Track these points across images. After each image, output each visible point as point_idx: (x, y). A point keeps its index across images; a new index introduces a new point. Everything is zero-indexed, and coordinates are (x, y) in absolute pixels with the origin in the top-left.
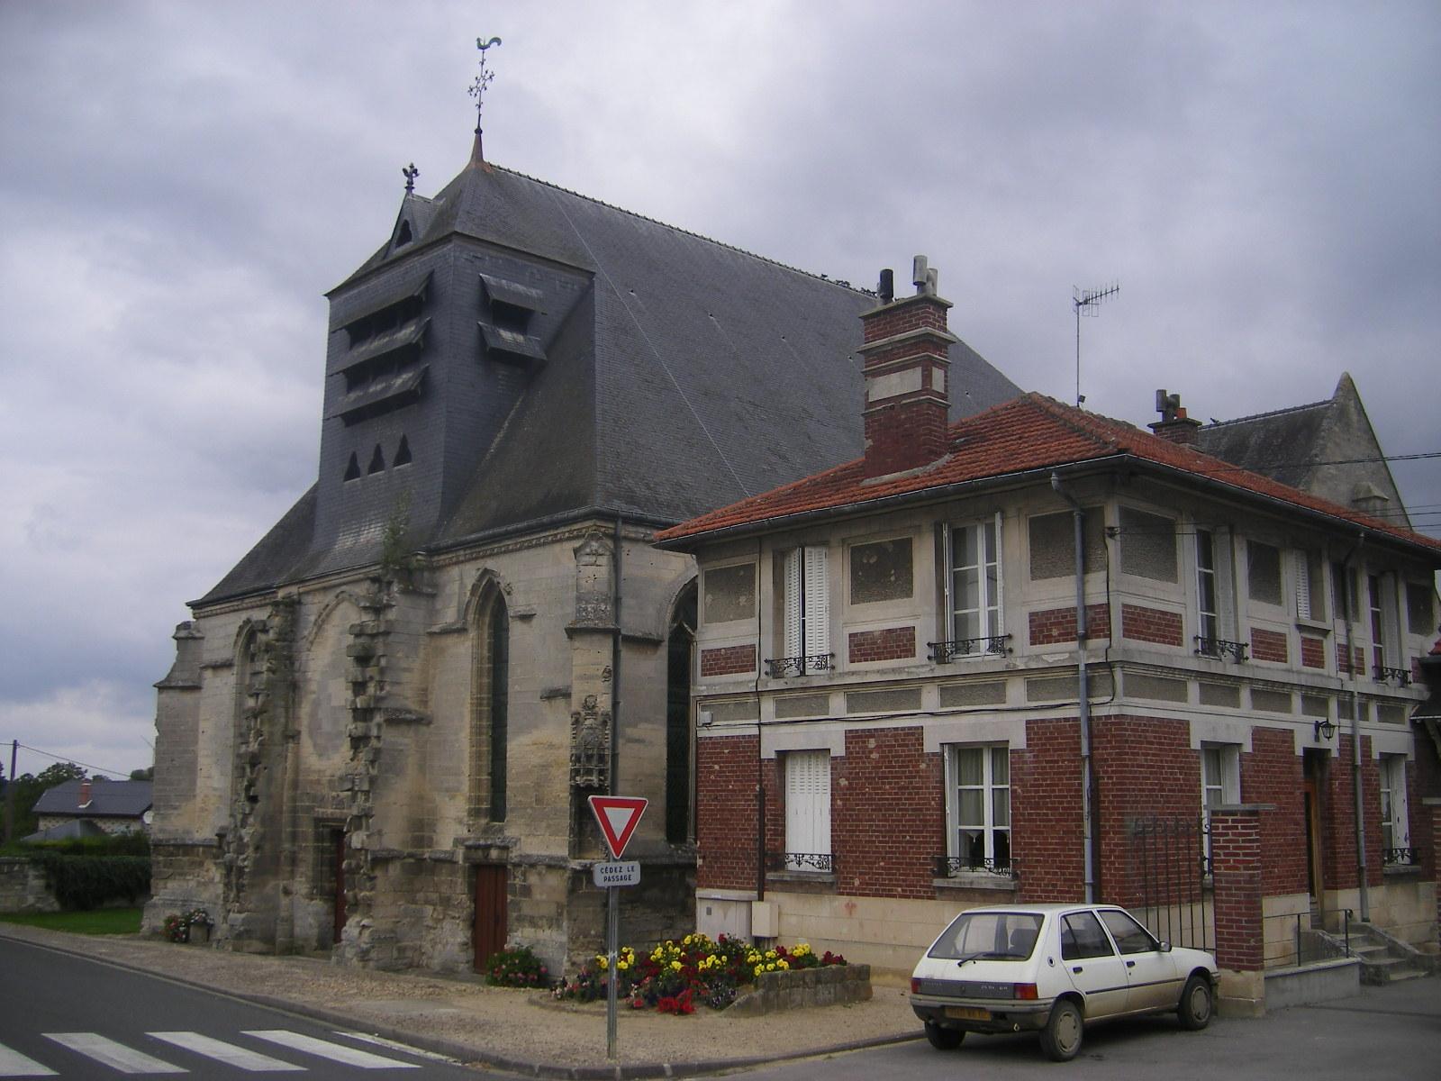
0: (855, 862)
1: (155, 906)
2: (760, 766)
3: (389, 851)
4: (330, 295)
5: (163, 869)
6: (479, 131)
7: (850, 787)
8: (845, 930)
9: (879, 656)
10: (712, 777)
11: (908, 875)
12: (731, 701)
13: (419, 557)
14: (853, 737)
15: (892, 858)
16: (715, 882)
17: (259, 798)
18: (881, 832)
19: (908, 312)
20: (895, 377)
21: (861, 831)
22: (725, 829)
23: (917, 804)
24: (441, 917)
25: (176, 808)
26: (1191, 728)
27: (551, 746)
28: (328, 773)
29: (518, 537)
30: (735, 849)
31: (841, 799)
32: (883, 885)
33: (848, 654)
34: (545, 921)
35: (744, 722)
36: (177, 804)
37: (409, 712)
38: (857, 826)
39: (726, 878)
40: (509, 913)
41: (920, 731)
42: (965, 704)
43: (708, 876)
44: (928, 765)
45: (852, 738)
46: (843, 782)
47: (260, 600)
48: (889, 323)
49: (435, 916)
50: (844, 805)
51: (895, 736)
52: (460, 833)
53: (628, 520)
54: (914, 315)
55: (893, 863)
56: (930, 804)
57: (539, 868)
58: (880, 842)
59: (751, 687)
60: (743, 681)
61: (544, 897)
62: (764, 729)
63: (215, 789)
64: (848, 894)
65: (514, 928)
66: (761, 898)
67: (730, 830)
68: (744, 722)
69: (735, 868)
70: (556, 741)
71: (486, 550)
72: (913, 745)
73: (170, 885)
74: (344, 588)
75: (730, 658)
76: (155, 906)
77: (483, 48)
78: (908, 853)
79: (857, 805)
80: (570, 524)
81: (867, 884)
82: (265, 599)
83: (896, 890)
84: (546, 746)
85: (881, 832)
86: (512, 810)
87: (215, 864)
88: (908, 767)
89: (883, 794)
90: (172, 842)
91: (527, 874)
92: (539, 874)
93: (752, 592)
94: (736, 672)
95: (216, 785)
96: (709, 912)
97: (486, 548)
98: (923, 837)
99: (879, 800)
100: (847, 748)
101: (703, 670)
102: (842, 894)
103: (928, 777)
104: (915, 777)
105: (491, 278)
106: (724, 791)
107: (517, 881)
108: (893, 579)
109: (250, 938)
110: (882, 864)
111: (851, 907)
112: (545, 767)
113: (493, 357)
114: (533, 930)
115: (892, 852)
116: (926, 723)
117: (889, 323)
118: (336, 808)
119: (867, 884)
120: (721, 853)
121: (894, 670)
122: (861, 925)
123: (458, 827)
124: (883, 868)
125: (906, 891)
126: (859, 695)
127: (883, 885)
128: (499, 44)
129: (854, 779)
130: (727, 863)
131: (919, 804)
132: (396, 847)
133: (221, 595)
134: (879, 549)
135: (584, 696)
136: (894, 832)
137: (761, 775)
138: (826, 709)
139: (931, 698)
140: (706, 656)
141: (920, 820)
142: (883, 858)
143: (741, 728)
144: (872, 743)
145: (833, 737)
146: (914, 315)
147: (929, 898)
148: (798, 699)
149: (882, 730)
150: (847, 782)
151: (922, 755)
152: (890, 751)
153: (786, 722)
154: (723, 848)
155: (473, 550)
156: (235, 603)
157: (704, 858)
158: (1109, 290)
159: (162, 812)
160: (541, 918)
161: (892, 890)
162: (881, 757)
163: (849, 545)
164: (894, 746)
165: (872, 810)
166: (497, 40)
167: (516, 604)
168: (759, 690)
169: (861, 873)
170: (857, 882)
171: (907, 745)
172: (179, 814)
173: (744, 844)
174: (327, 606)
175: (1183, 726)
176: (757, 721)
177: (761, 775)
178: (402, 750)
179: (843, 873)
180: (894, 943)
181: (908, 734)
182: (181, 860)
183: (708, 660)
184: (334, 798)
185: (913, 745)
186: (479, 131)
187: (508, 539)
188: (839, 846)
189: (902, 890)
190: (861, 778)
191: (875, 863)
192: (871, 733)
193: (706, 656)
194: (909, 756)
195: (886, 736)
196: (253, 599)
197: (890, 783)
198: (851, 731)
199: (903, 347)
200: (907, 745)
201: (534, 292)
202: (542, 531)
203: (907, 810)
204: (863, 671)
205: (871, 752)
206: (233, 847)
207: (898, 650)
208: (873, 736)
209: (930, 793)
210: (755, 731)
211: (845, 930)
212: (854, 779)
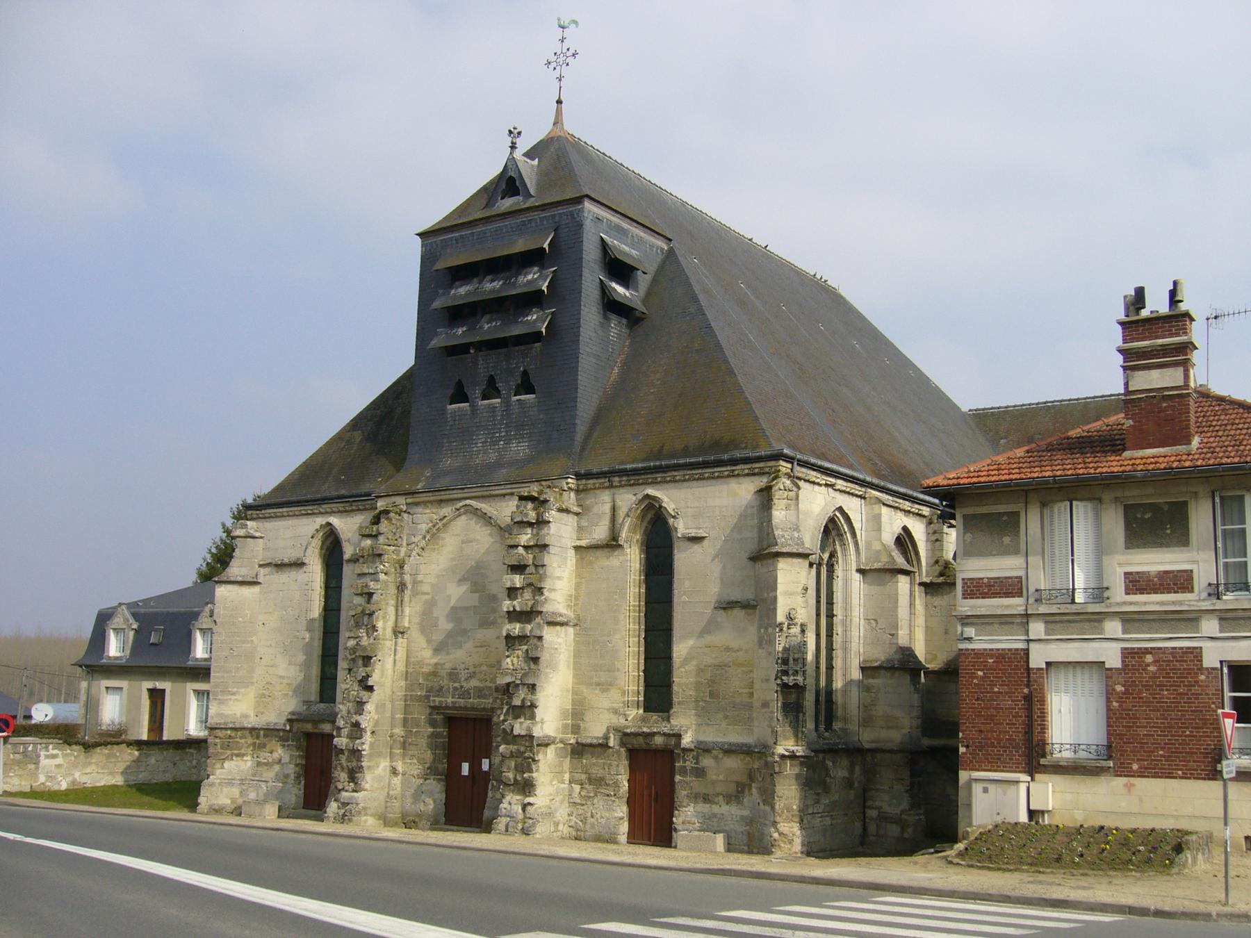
0: (1131, 751)
1: (212, 785)
2: (1028, 674)
3: (548, 737)
4: (421, 235)
5: (220, 751)
6: (559, 102)
7: (1126, 692)
8: (1123, 804)
9: (1155, 591)
10: (975, 681)
11: (1189, 761)
12: (996, 620)
13: (569, 480)
14: (1129, 653)
15: (1171, 748)
16: (980, 766)
17: (375, 688)
18: (1160, 727)
19: (1168, 323)
20: (1155, 373)
21: (1138, 727)
22: (990, 724)
23: (1196, 707)
24: (592, 795)
25: (234, 694)
26: (1204, 654)
27: (728, 649)
28: (448, 666)
29: (688, 469)
30: (1002, 740)
31: (1117, 702)
32: (1162, 769)
33: (1123, 588)
34: (721, 797)
35: (1010, 638)
36: (235, 690)
37: (561, 615)
38: (1134, 723)
39: (992, 762)
40: (677, 791)
41: (1199, 650)
42: (1244, 631)
43: (971, 762)
44: (1208, 677)
45: (1127, 654)
46: (1119, 688)
47: (344, 507)
48: (1147, 329)
49: (583, 794)
50: (1120, 706)
51: (1171, 653)
52: (613, 721)
53: (804, 464)
54: (1175, 326)
55: (1172, 752)
56: (1210, 707)
57: (715, 752)
58: (1158, 735)
59: (1021, 610)
60: (1014, 605)
61: (721, 777)
62: (1033, 646)
63: (281, 677)
64: (1125, 776)
65: (685, 804)
66: (1033, 780)
67: (995, 724)
68: (1010, 638)
69: (1002, 755)
70: (734, 645)
71: (638, 480)
72: (1191, 661)
73: (226, 764)
74: (468, 502)
75: (994, 586)
76: (212, 785)
77: (563, 27)
78: (1189, 744)
79: (1133, 706)
80: (752, 463)
81: (1146, 768)
82: (352, 505)
83: (1176, 773)
84: (722, 649)
85: (1160, 727)
86: (679, 703)
87: (283, 746)
88: (1187, 678)
89: (1160, 698)
90: (231, 726)
91: (700, 758)
92: (716, 758)
93: (1017, 533)
94: (1000, 597)
95: (281, 673)
96: (985, 790)
97: (649, 476)
98: (1204, 732)
99: (1157, 703)
100: (1123, 662)
101: (963, 594)
102: (1120, 776)
103: (1208, 686)
104: (1194, 686)
105: (608, 238)
106: (988, 693)
107: (688, 763)
108: (1168, 531)
109: (366, 814)
110: (1161, 752)
111: (1129, 787)
112: (720, 666)
113: (612, 306)
114: (708, 806)
115: (1172, 744)
116: (1206, 645)
117: (1147, 329)
118: (459, 698)
119: (1146, 768)
120: (986, 743)
121: (1174, 603)
122: (1141, 800)
123: (612, 716)
124: (1162, 756)
125: (1186, 774)
126: (1131, 620)
127: (1162, 769)
128: (577, 27)
129: (1129, 686)
130: (993, 751)
131: (1198, 707)
132: (552, 734)
133: (272, 501)
134: (1154, 507)
135: (787, 609)
136: (1173, 727)
137: (1029, 681)
138: (1102, 631)
139: (1210, 626)
140: (966, 583)
141: (1199, 719)
142: (1163, 749)
143: (1008, 642)
144: (1149, 658)
145: (1112, 656)
146: (1175, 326)
147: (1210, 779)
148: (1069, 621)
149: (1160, 649)
150: (1123, 689)
151: (1201, 669)
152: (1167, 665)
153: (1057, 639)
154: (988, 739)
155: (632, 478)
156: (310, 508)
157: (967, 747)
158: (1226, 313)
159: (219, 697)
160: (718, 795)
161: (1173, 773)
162: (1158, 670)
163: (1122, 502)
164: (1172, 661)
165: (1150, 710)
166: (575, 22)
167: (682, 527)
168: (1029, 613)
169: (1138, 760)
170: (1135, 767)
171: (1186, 661)
172: (236, 700)
173: (1012, 736)
174: (445, 517)
175: (1197, 654)
176: (1025, 638)
177: (1029, 681)
178: (556, 649)
179: (1120, 759)
180: (1175, 813)
181: (1186, 653)
182: (238, 742)
183: (969, 587)
184: (455, 689)
185: (1191, 661)
186: (559, 102)
187: (675, 471)
188: (1115, 739)
189: (1183, 773)
190: (1137, 686)
191: (1153, 752)
192: (1147, 651)
193: (966, 583)
194: (1189, 669)
195: (1164, 653)
196: (335, 505)
197: (1167, 690)
198: (1125, 649)
199: (1162, 350)
200: (1186, 661)
201: (634, 252)
202: (717, 466)
203: (1187, 711)
204: (1142, 603)
205: (1148, 665)
206: (345, 732)
207: (1175, 587)
208: (1151, 653)
209: (1209, 699)
210: (1021, 646)
211: (1123, 804)
212: (1129, 686)
